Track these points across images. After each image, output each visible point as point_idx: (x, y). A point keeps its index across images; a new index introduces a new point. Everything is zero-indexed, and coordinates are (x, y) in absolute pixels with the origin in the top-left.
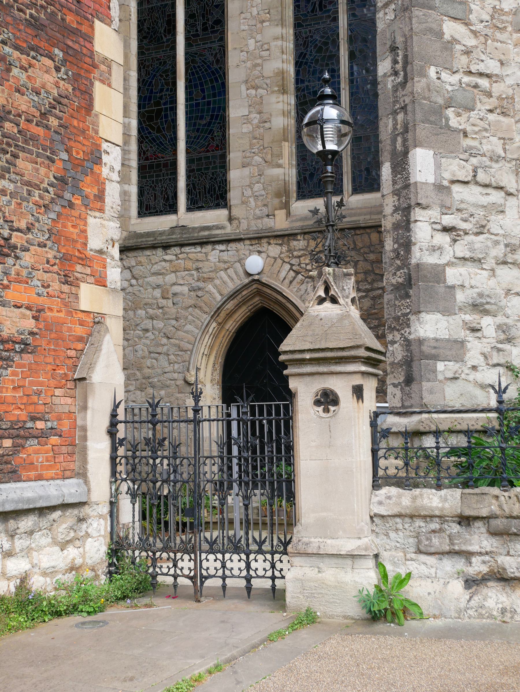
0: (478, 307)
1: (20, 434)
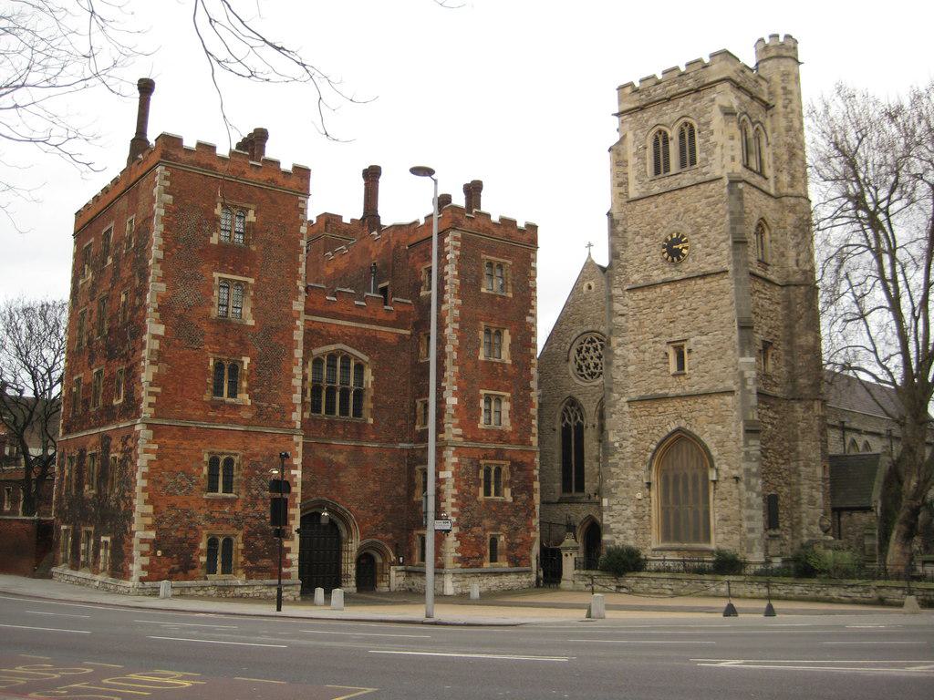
0: (619, 533)
1: (520, 559)
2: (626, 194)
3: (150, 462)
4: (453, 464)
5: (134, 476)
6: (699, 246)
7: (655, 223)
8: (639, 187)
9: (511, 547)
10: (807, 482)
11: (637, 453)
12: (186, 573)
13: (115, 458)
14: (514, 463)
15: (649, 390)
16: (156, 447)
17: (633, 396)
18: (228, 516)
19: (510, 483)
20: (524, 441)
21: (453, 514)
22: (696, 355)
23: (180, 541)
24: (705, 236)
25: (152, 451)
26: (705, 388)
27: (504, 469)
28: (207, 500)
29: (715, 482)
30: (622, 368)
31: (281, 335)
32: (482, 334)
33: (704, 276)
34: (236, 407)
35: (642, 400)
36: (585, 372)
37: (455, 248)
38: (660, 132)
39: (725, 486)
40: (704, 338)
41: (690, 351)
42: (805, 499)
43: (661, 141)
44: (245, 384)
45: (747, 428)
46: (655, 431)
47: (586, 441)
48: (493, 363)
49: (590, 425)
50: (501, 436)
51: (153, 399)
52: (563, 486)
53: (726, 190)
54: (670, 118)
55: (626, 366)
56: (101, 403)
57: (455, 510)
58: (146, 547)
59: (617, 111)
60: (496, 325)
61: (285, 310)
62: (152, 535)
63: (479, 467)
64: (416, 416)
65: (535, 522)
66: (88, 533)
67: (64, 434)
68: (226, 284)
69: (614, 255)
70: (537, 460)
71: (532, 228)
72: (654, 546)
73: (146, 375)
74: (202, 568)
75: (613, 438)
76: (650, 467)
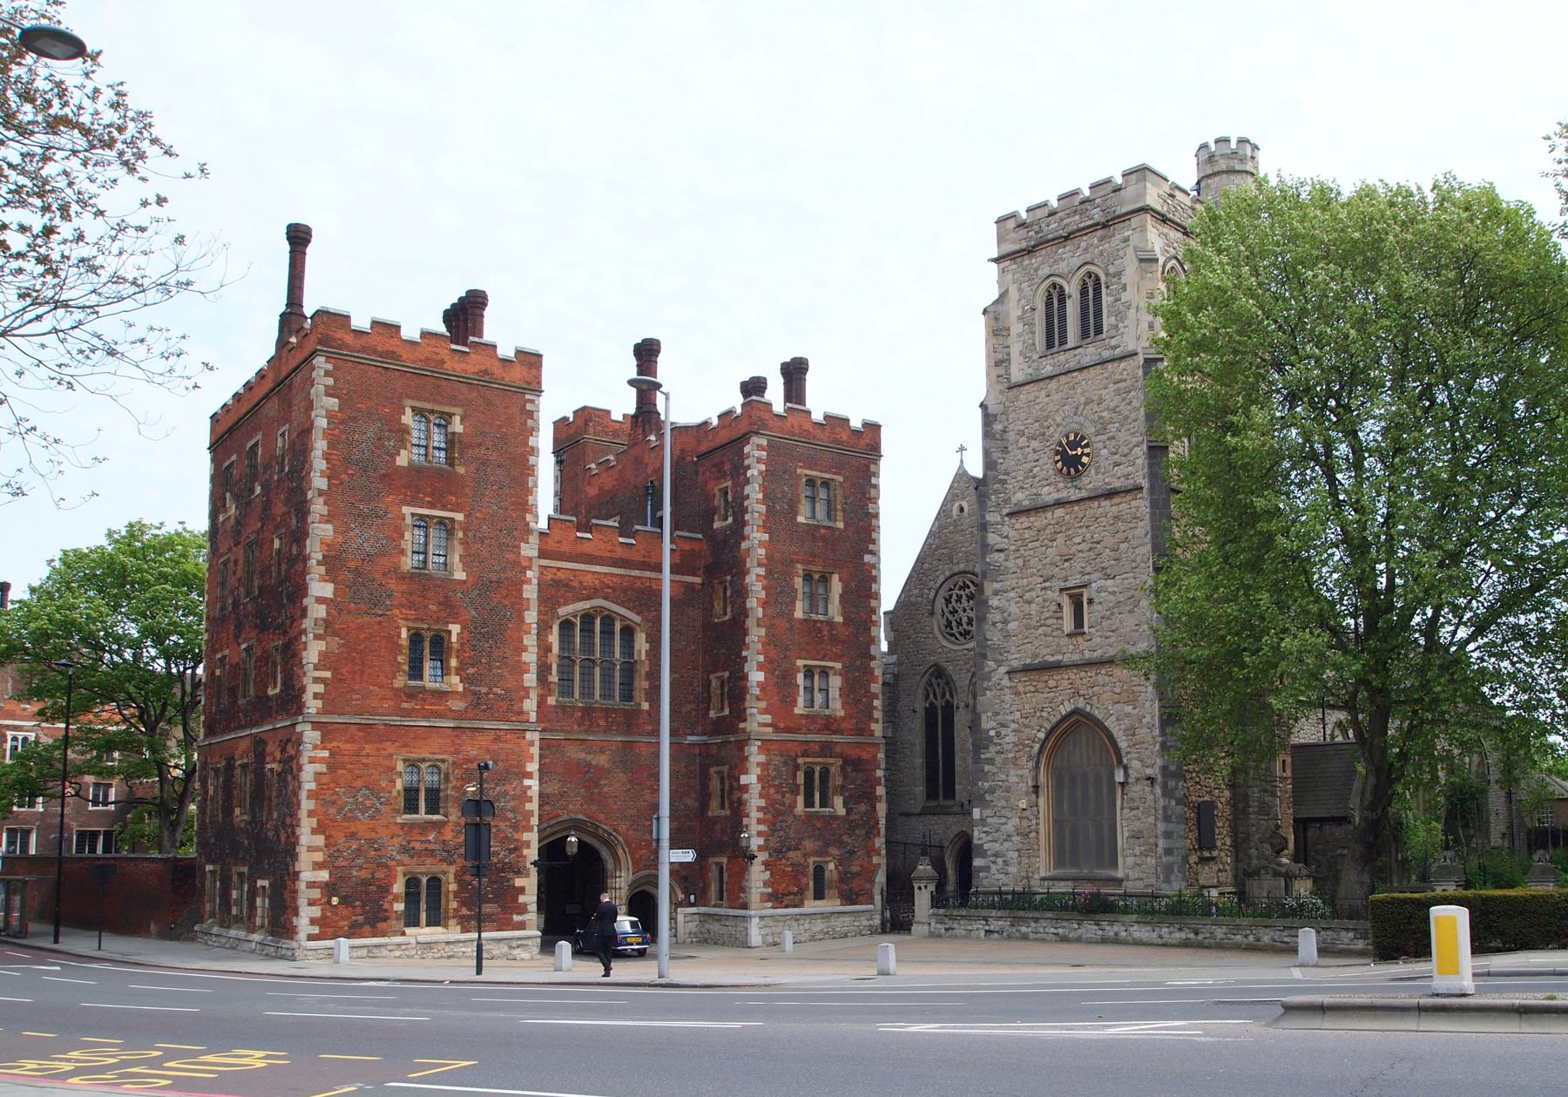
3: (318, 775)
4: (759, 764)
5: (296, 794)
6: (1104, 452)
7: (1046, 418)
8: (1025, 366)
9: (844, 877)
11: (1020, 745)
12: (373, 926)
13: (272, 770)
14: (847, 761)
15: (1037, 656)
16: (326, 754)
17: (1015, 664)
18: (432, 847)
19: (842, 790)
20: (862, 730)
21: (760, 834)
22: (1099, 607)
23: (366, 883)
24: (1113, 438)
25: (322, 760)
26: (1111, 652)
27: (832, 769)
28: (403, 825)
30: (1000, 625)
31: (504, 592)
32: (798, 582)
33: (1110, 494)
34: (441, 695)
35: (1027, 669)
36: (955, 630)
37: (759, 460)
38: (1054, 285)
40: (1110, 582)
41: (1090, 601)
43: (1055, 298)
44: (454, 663)
46: (1045, 714)
47: (957, 726)
48: (815, 621)
49: (962, 705)
50: (829, 724)
51: (320, 688)
52: (928, 789)
53: (1140, 372)
54: (1068, 263)
55: (1005, 622)
56: (252, 692)
57: (763, 828)
58: (316, 893)
60: (819, 568)
61: (511, 556)
62: (324, 875)
63: (797, 767)
64: (709, 698)
65: (880, 842)
66: (241, 875)
67: (206, 736)
68: (423, 522)
69: (989, 464)
70: (881, 756)
71: (873, 429)
72: (1043, 874)
73: (313, 651)
74: (398, 919)
75: (987, 723)
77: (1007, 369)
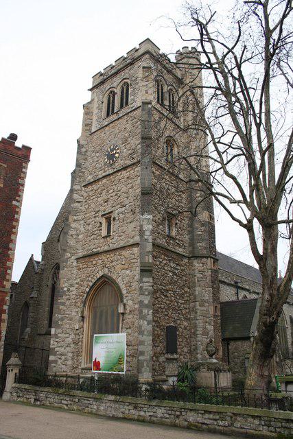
2: (90, 130)
10: (202, 317)
17: (80, 255)
26: (122, 244)
29: (123, 314)
30: (75, 236)
33: (125, 168)
35: (84, 257)
39: (129, 318)
42: (200, 330)
45: (142, 268)
46: (90, 279)
55: (78, 235)
59: (91, 87)
70: (8, 298)
71: (27, 150)
72: (83, 366)
76: (84, 306)
77: (91, 127)
